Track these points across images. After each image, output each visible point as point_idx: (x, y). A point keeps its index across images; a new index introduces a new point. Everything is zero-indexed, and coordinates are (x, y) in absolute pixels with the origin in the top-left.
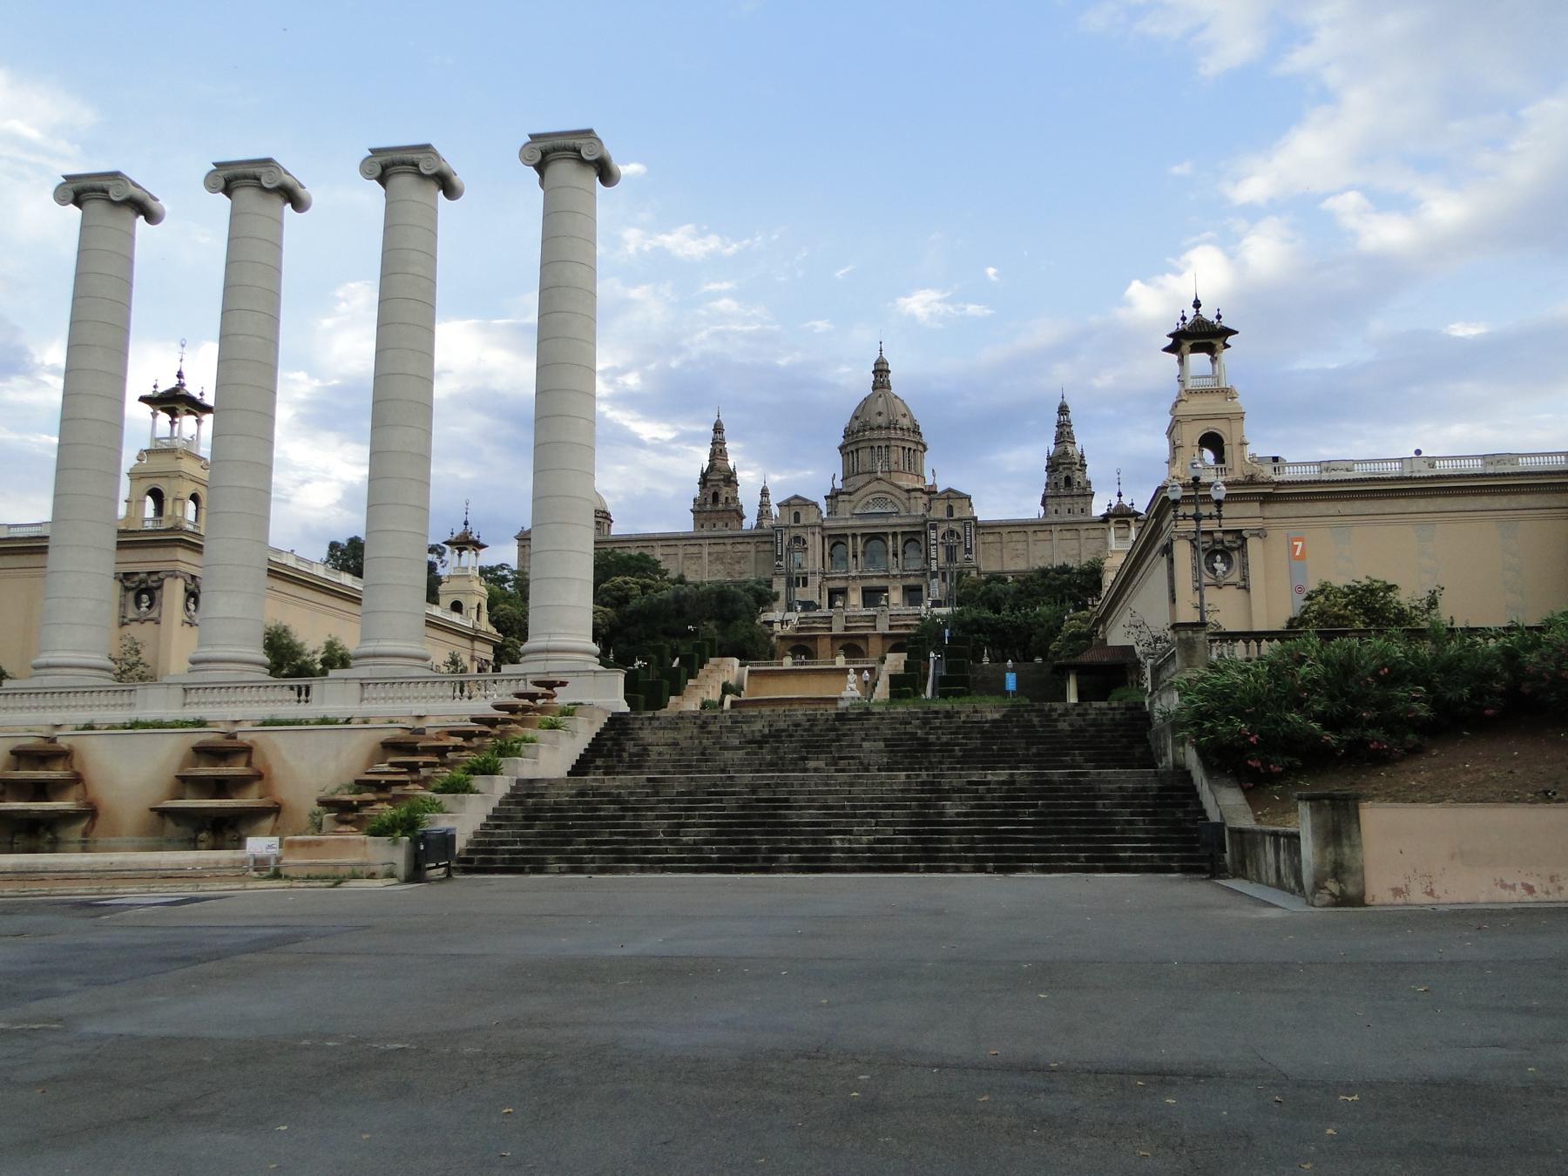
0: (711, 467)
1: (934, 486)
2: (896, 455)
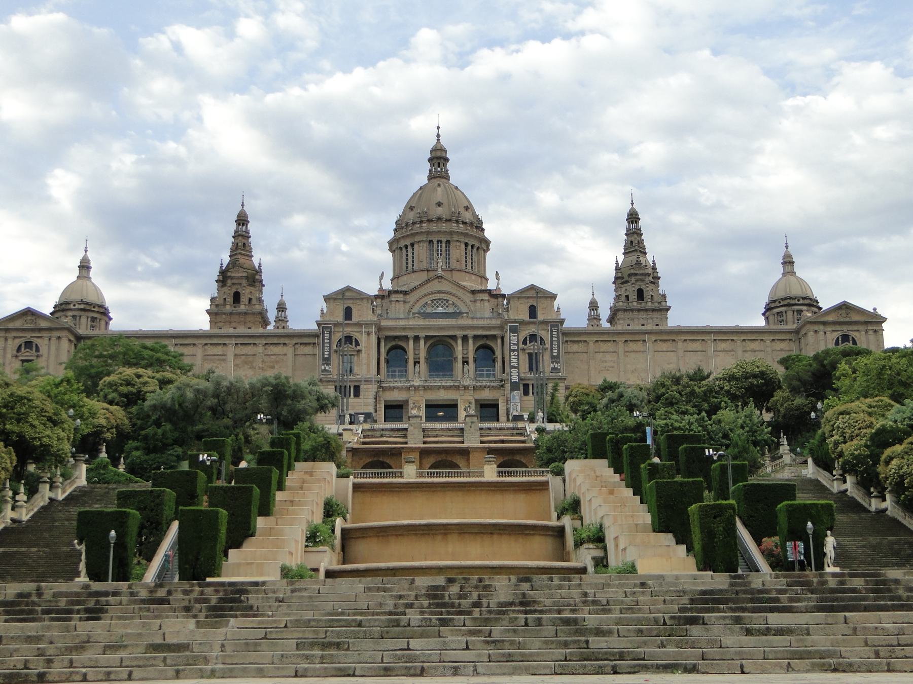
0: (233, 263)
1: (498, 289)
2: (457, 252)
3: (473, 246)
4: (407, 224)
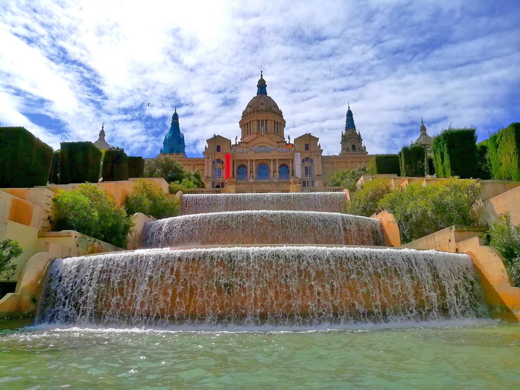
3: (278, 123)
4: (247, 113)
